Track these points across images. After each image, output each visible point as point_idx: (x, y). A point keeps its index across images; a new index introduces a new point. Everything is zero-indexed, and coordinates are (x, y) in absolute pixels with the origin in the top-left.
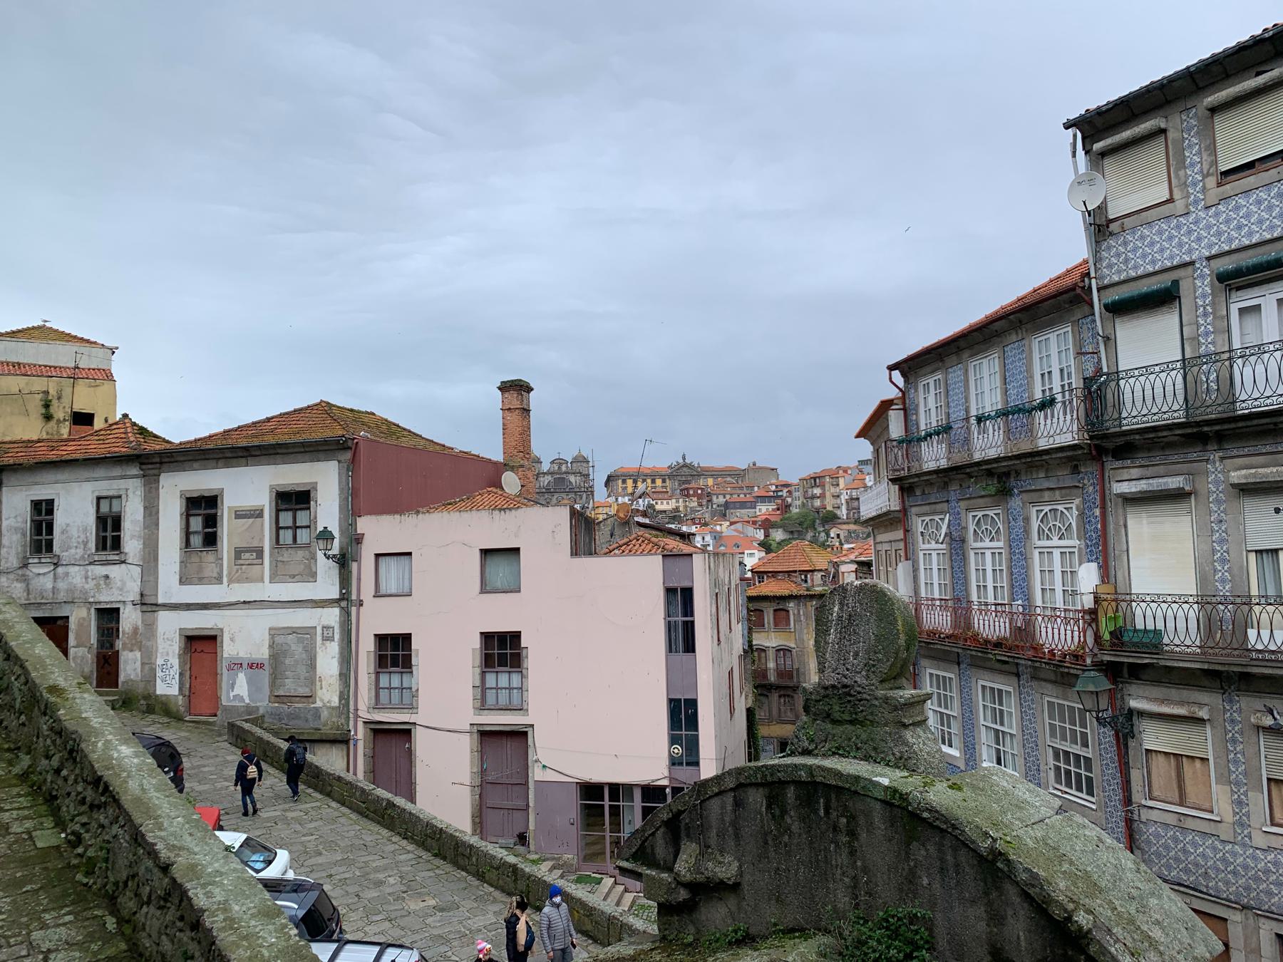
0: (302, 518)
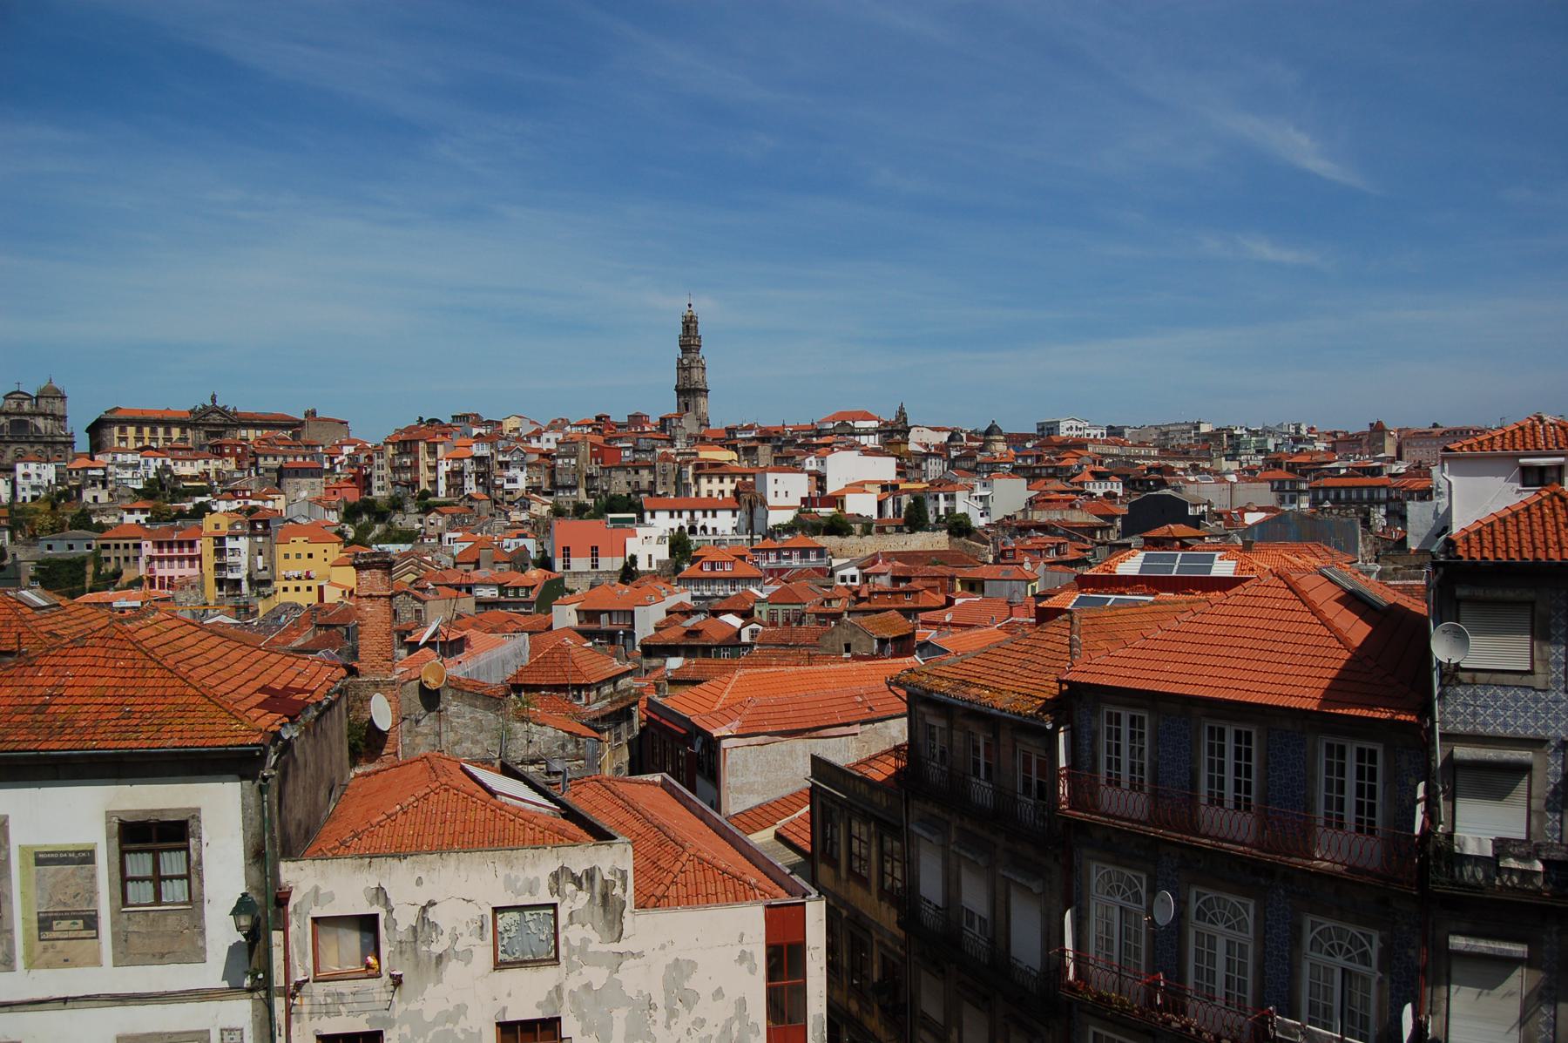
0: (172, 863)
